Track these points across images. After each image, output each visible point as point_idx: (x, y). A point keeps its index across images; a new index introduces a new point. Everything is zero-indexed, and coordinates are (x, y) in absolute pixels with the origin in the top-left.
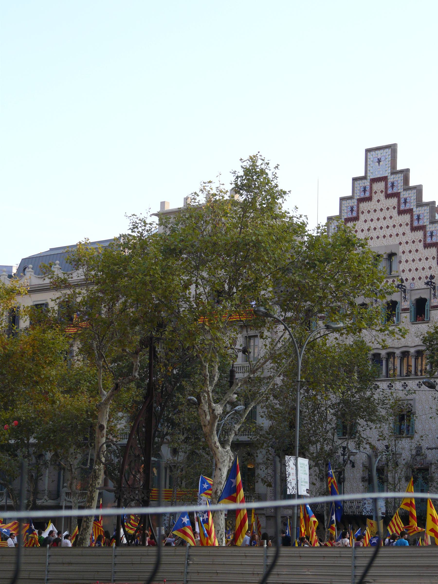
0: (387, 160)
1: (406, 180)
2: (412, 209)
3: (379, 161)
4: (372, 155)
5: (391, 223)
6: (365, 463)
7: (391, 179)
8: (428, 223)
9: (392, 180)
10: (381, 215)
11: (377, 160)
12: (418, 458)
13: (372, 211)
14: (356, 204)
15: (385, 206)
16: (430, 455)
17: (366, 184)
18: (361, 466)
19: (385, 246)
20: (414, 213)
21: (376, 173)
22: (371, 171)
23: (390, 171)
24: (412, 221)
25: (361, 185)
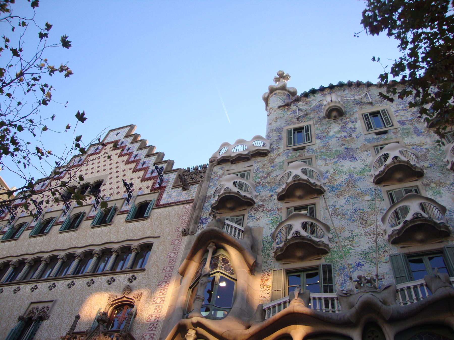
3: (118, 134)
11: (116, 134)
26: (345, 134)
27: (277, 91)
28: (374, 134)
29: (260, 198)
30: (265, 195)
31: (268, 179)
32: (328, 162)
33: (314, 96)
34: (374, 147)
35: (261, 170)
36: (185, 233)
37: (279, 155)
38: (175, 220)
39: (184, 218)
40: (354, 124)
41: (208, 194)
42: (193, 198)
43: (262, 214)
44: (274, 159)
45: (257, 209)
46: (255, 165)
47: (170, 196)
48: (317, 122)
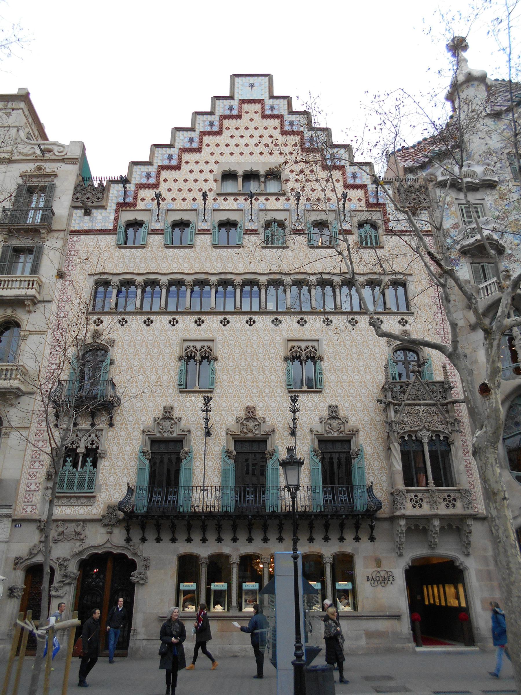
0: (264, 86)
2: (302, 132)
3: (252, 86)
4: (242, 80)
6: (232, 429)
7: (269, 102)
9: (271, 103)
11: (248, 85)
12: (335, 423)
13: (242, 128)
15: (261, 125)
16: (354, 419)
17: (232, 104)
18: (224, 434)
19: (264, 163)
21: (248, 95)
46: (486, 199)
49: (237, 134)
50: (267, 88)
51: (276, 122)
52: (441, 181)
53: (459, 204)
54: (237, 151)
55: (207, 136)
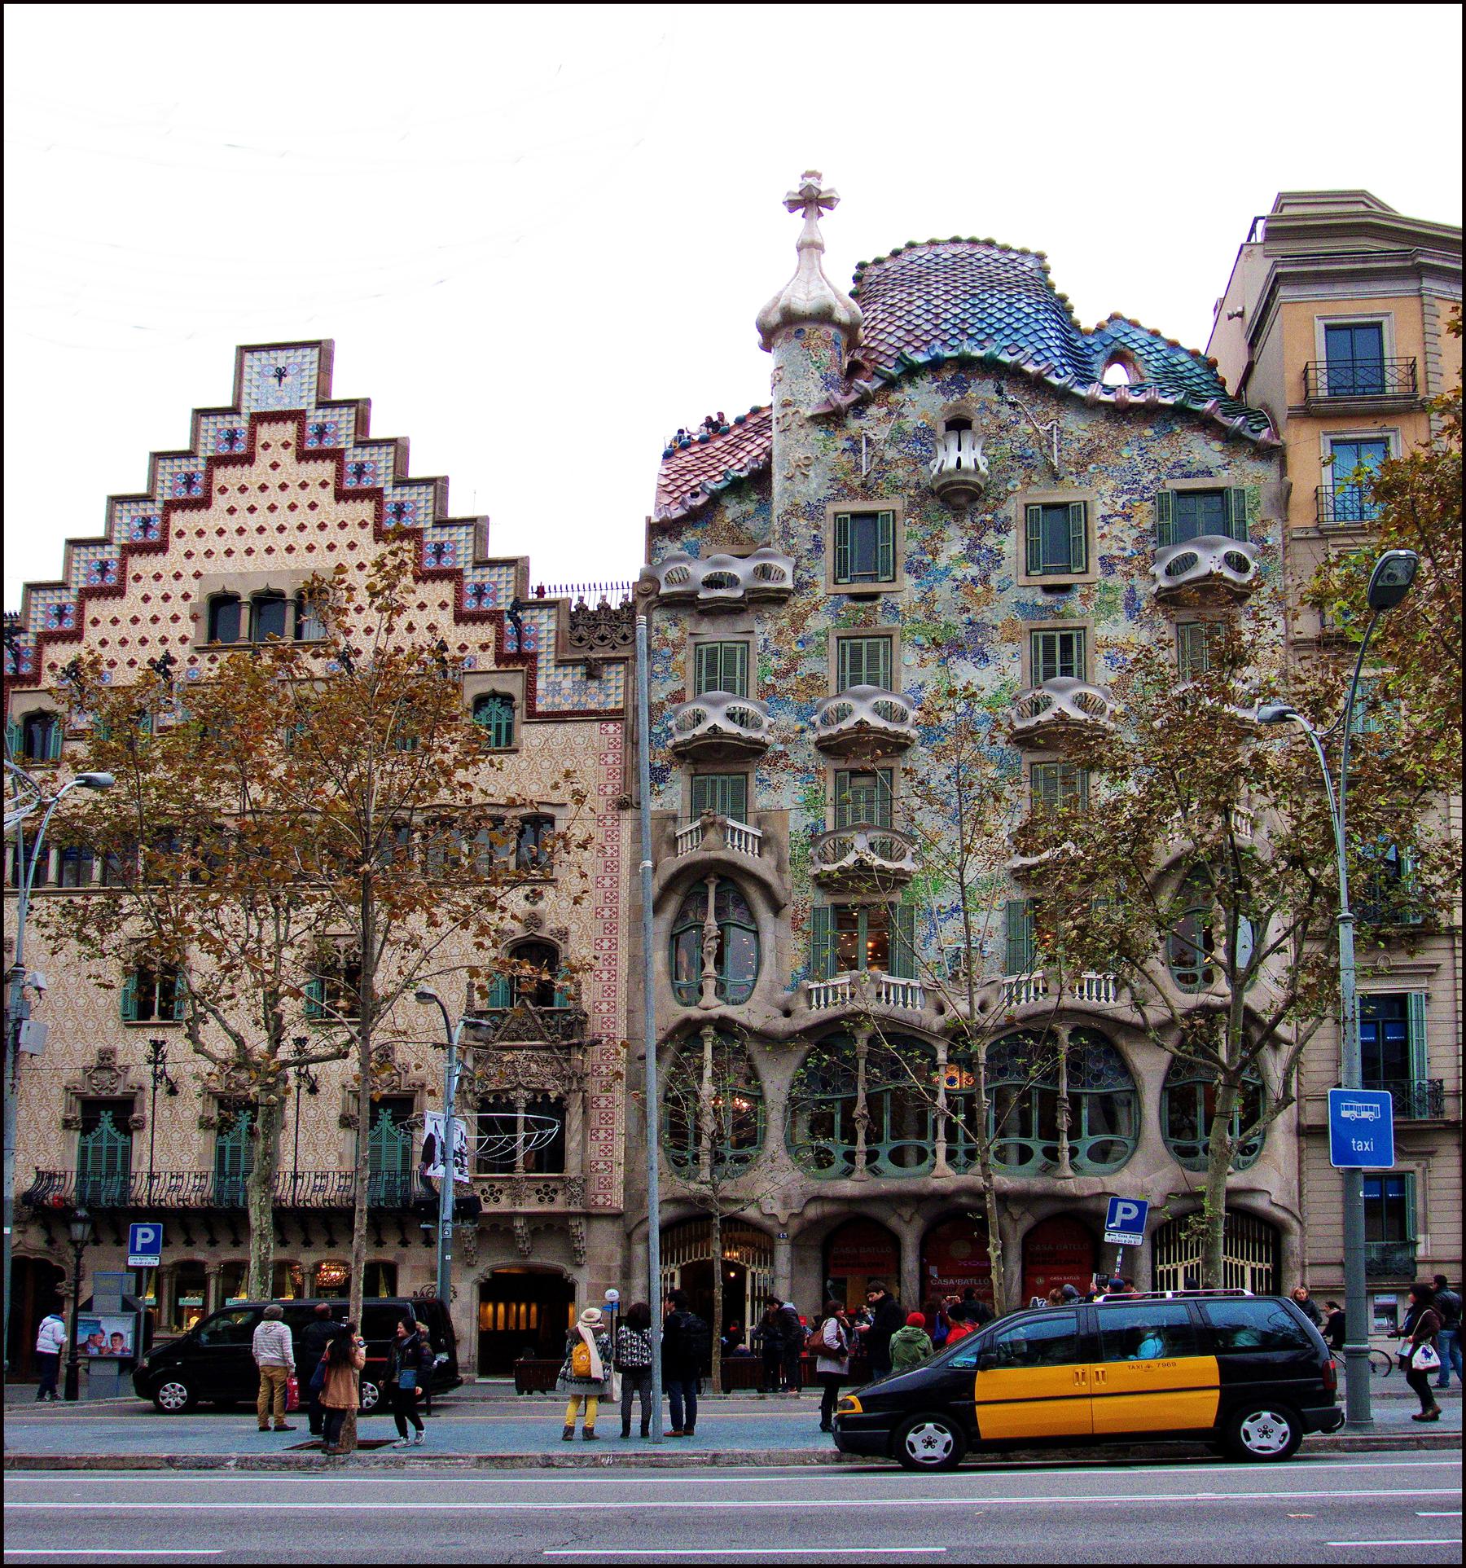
0: (307, 373)
1: (362, 423)
5: (312, 519)
7: (316, 417)
8: (430, 525)
9: (320, 420)
10: (283, 500)
11: (273, 372)
13: (253, 488)
14: (202, 468)
15: (293, 478)
17: (235, 425)
19: (293, 571)
20: (386, 500)
22: (254, 396)
23: (313, 400)
24: (379, 517)
25: (219, 426)
26: (973, 571)
27: (807, 328)
28: (1039, 590)
29: (777, 733)
30: (788, 727)
31: (792, 681)
32: (926, 656)
33: (911, 382)
34: (1032, 631)
35: (773, 646)
36: (623, 805)
37: (815, 608)
38: (590, 762)
39: (610, 759)
40: (1002, 537)
41: (655, 700)
42: (620, 706)
43: (785, 777)
44: (803, 617)
45: (773, 762)
46: (758, 629)
47: (555, 688)
48: (913, 505)
49: (242, 502)
50: (315, 379)
51: (327, 469)
52: (666, 596)
53: (697, 644)
54: (239, 544)
55: (179, 512)
